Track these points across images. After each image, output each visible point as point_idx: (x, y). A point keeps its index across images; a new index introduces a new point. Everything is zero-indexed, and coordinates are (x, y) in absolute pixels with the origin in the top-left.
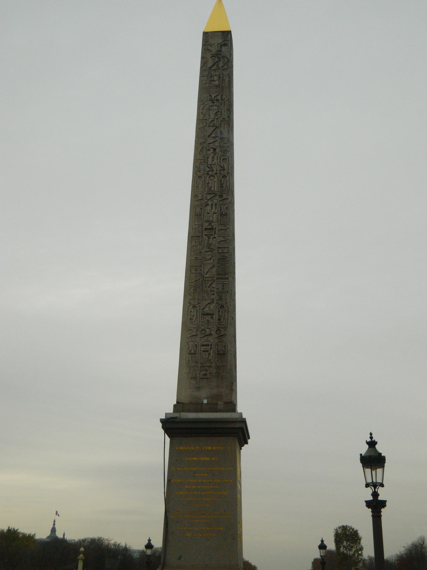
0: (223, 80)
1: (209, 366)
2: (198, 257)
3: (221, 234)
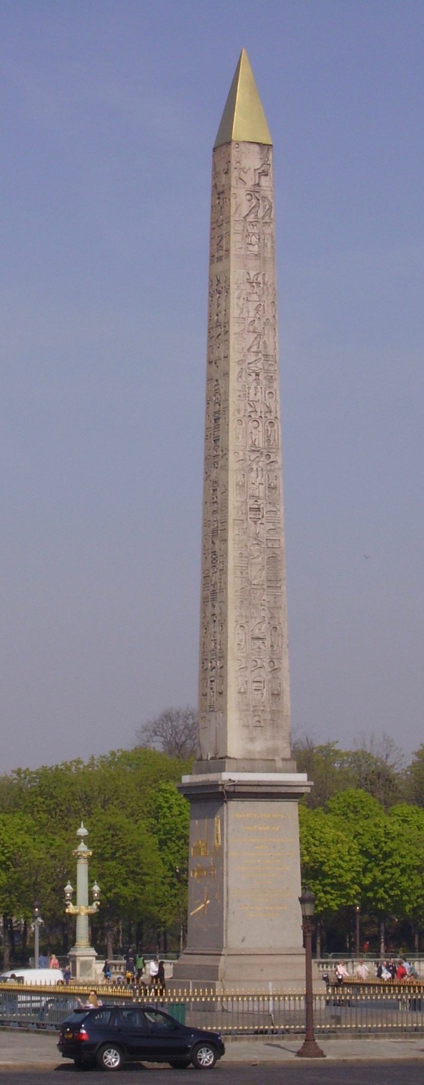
0: (265, 245)
1: (263, 710)
3: (269, 518)
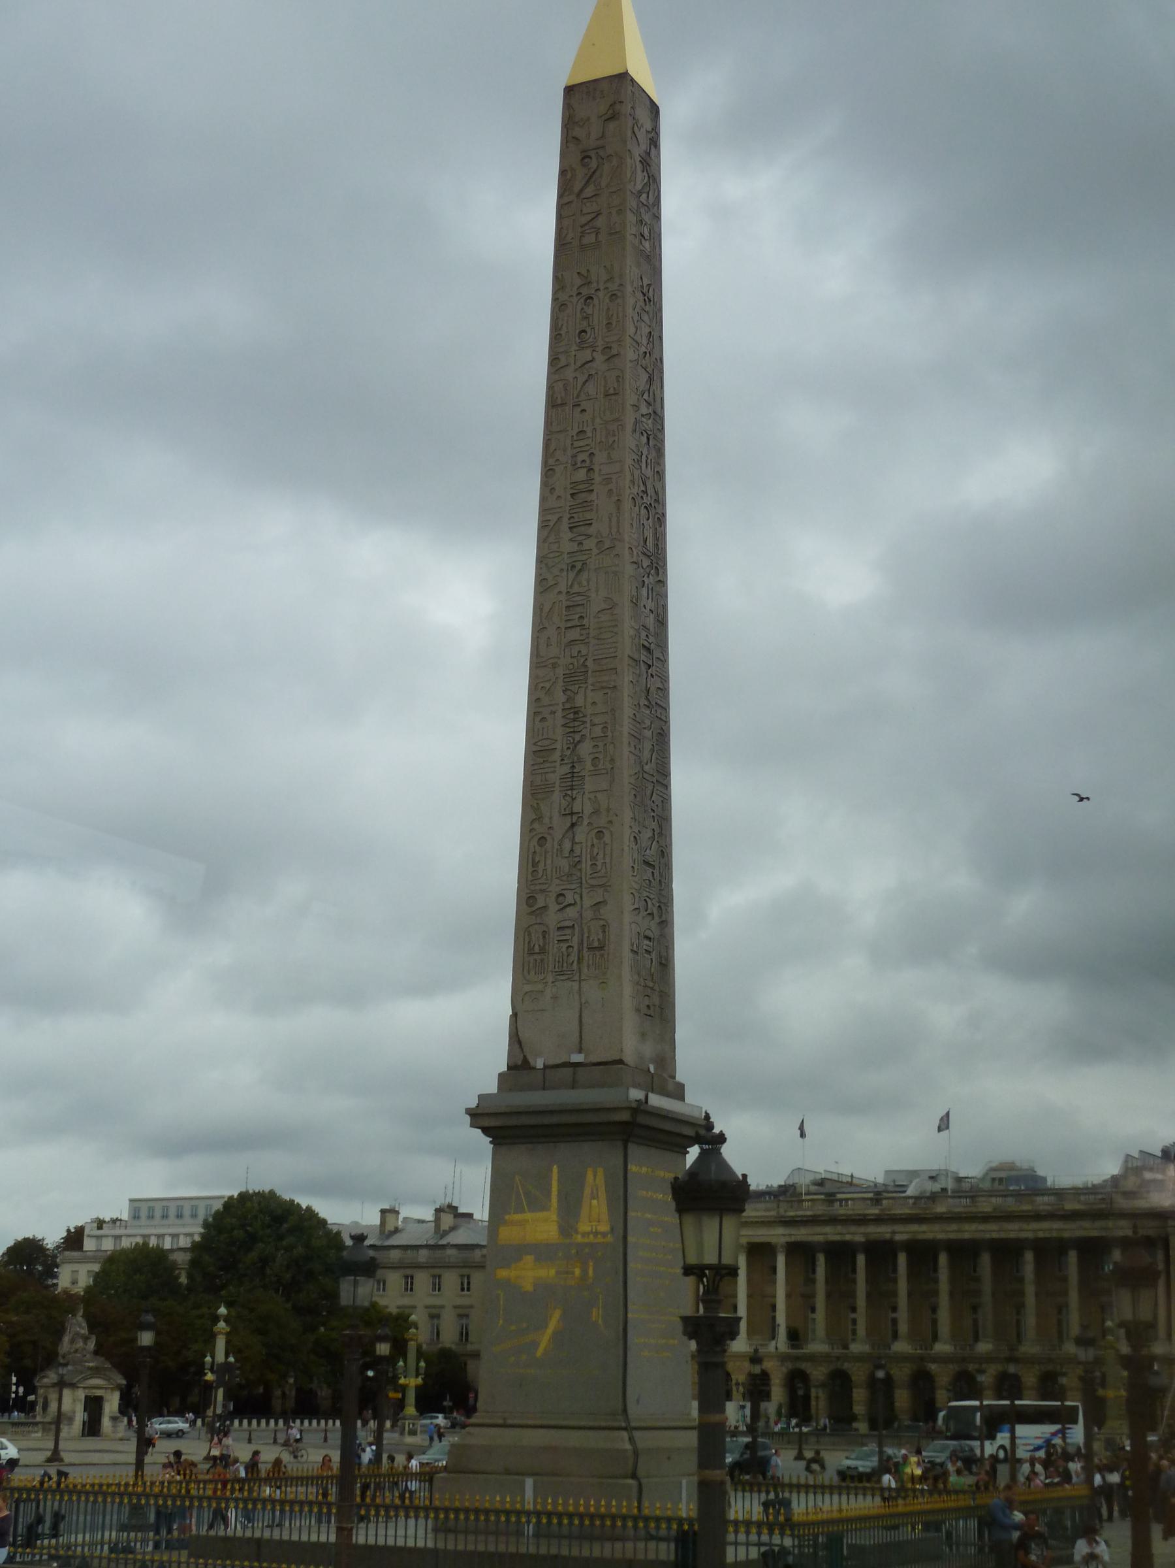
2: (637, 714)
